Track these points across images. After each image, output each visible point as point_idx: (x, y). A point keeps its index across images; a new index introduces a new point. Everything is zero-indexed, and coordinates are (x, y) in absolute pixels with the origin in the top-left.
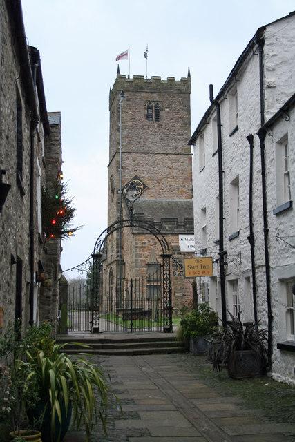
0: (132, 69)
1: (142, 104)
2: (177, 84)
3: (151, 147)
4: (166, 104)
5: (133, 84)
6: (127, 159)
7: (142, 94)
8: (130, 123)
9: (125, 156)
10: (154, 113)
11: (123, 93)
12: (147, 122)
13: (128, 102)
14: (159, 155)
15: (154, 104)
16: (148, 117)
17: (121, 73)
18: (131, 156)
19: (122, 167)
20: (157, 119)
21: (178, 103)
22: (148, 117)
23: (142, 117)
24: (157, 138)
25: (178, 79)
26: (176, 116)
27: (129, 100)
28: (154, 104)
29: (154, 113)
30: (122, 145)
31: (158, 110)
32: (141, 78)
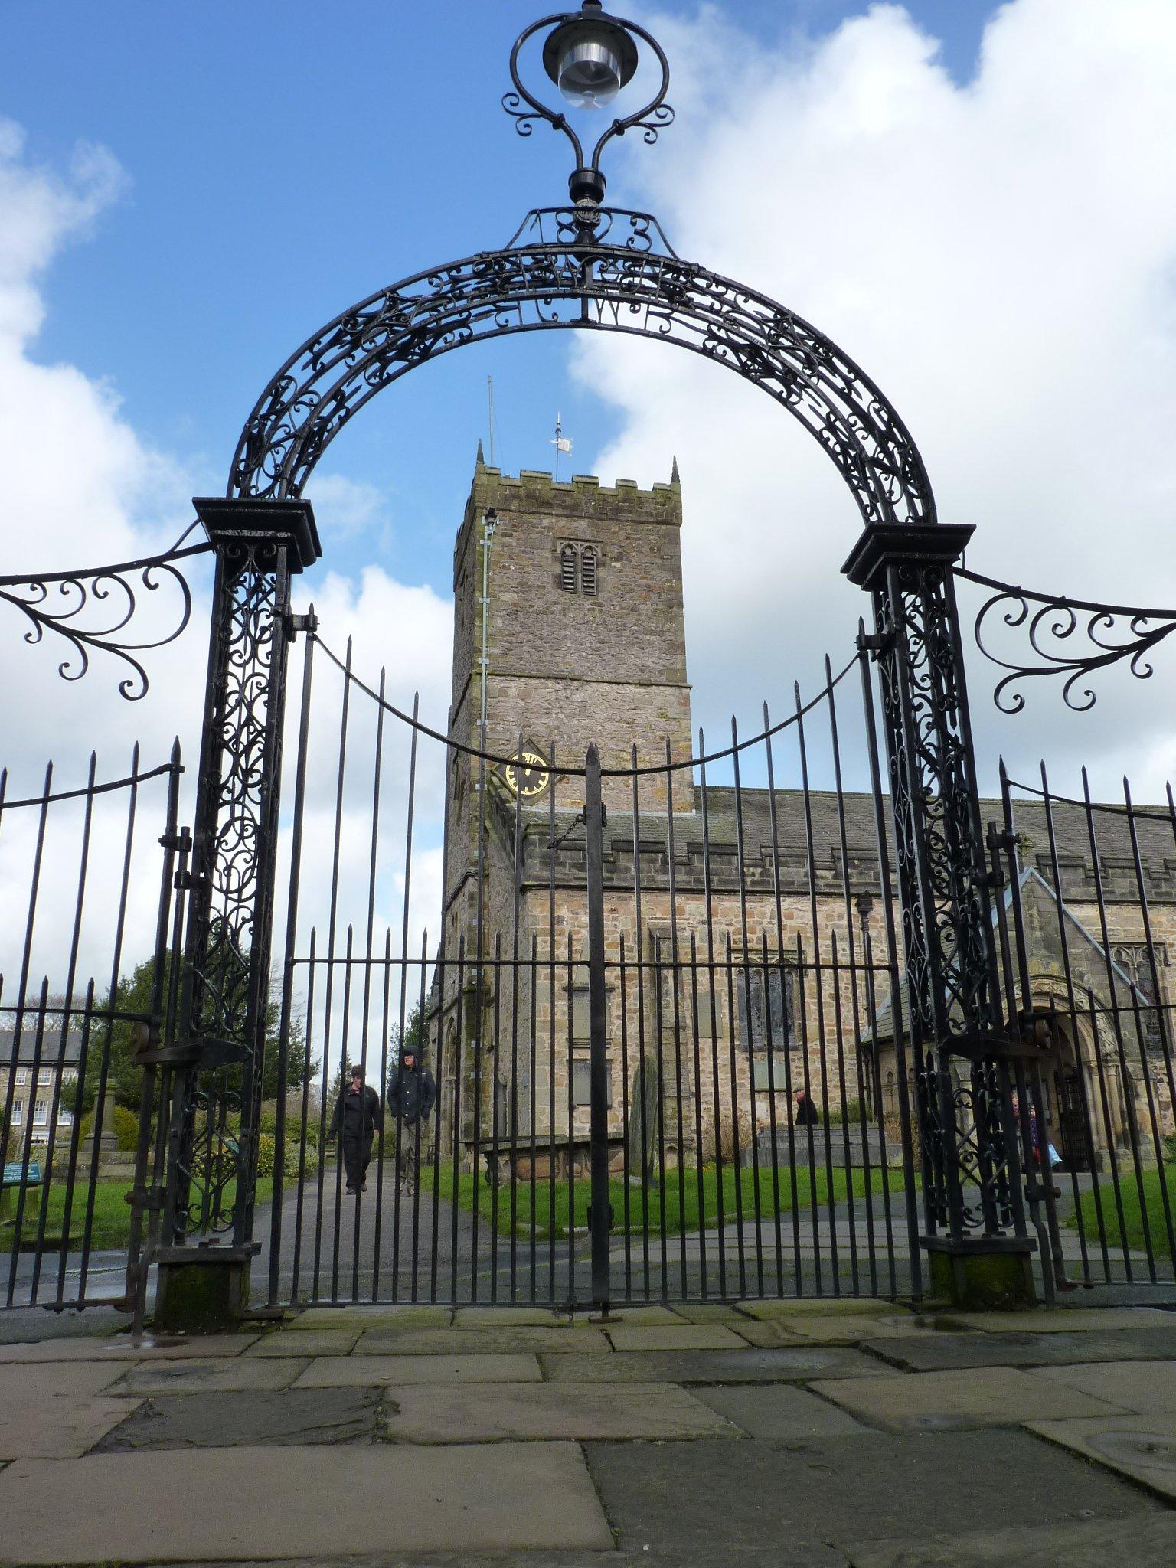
0: (512, 467)
1: (548, 546)
2: (642, 498)
3: (573, 663)
5: (522, 492)
6: (503, 693)
7: (546, 521)
8: (509, 597)
9: (497, 684)
10: (578, 573)
11: (491, 514)
12: (556, 594)
13: (508, 539)
14: (595, 686)
15: (579, 548)
16: (563, 582)
17: (487, 462)
18: (513, 687)
19: (488, 716)
20: (591, 585)
21: (646, 549)
22: (563, 582)
23: (549, 581)
24: (589, 640)
25: (645, 485)
26: (641, 582)
27: (511, 536)
28: (579, 548)
29: (578, 573)
30: (488, 656)
31: (590, 567)
32: (546, 478)
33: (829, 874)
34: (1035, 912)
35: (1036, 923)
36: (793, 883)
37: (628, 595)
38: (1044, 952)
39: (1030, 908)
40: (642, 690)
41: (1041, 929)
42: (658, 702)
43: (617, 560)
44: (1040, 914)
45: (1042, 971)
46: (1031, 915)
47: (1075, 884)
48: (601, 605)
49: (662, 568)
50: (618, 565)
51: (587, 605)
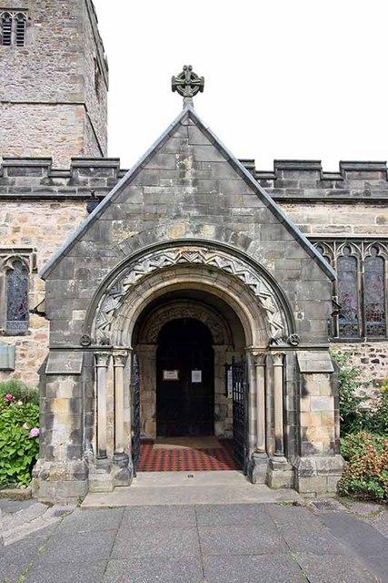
4: (36, 17)
26: (55, 36)
33: (64, 181)
34: (189, 163)
35: (189, 176)
36: (29, 190)
37: (45, 46)
38: (195, 212)
39: (183, 158)
40: (51, 107)
41: (195, 183)
42: (61, 115)
43: (38, 22)
44: (195, 166)
45: (190, 236)
46: (183, 167)
47: (309, 186)
48: (26, 53)
49: (70, 26)
50: (39, 25)
51: (17, 53)
